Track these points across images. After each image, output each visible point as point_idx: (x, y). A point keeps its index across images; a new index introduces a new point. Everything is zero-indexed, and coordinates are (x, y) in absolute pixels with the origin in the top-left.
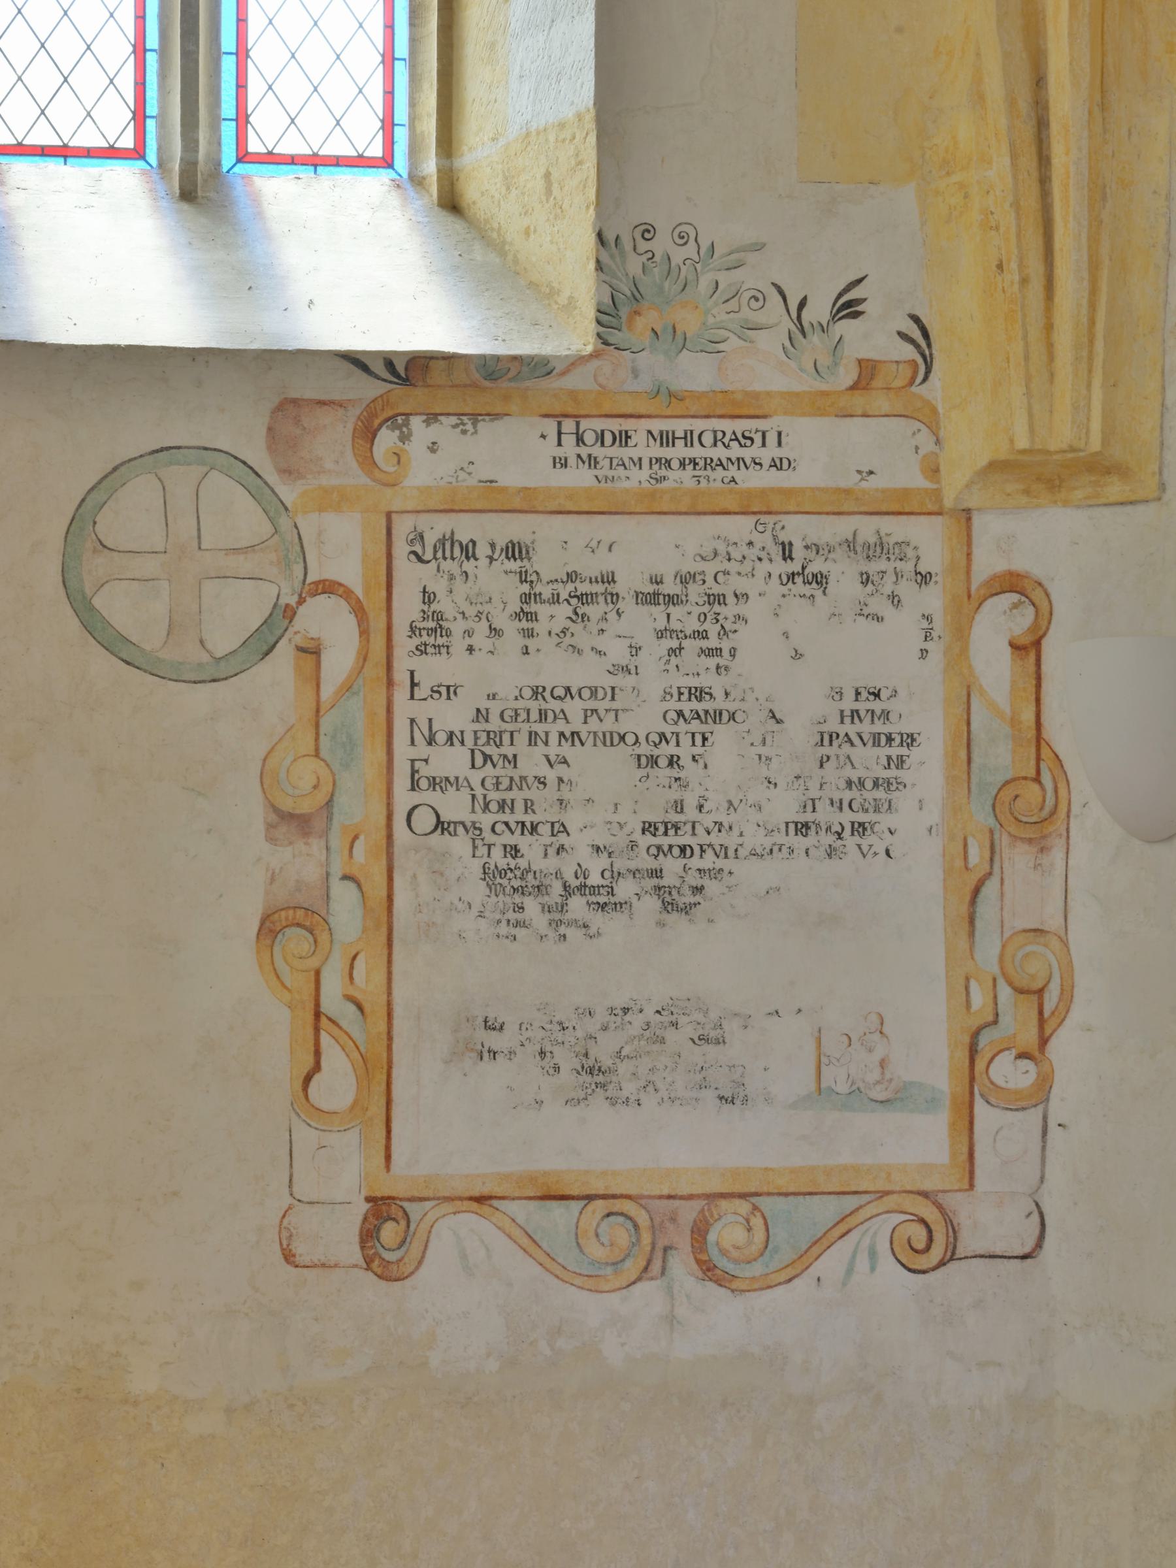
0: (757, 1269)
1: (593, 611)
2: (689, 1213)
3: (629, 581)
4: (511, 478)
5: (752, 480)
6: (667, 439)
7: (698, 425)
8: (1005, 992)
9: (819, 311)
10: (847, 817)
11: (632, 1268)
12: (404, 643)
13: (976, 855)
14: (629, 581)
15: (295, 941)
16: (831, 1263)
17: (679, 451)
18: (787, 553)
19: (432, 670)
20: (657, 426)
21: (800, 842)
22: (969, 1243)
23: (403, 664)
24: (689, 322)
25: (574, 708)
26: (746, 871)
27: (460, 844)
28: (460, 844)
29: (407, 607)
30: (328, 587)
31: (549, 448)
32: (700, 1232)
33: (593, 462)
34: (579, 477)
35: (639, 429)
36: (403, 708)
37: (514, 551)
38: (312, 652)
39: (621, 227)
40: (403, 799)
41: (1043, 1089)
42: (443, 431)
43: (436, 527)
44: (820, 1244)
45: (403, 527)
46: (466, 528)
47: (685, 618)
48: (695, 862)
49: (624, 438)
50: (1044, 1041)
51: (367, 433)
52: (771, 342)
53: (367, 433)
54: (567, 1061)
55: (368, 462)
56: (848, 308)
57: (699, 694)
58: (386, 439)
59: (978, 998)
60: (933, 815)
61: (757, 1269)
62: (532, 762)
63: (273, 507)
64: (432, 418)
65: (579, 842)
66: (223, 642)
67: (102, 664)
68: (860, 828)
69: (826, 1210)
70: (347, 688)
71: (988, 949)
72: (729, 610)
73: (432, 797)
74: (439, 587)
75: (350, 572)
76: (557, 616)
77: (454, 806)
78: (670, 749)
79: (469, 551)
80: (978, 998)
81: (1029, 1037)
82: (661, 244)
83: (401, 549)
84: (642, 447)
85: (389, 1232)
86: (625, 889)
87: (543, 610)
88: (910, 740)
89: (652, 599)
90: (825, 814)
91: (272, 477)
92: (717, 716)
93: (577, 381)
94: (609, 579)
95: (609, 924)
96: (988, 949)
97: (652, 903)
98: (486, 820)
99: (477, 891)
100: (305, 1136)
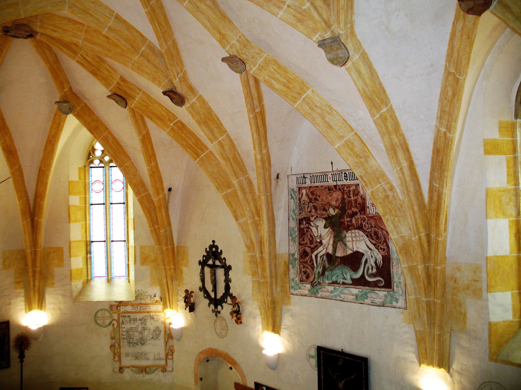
0: (150, 372)
1: (135, 321)
2: (144, 368)
3: (138, 319)
4: (129, 310)
5: (148, 310)
6: (141, 307)
7: (143, 306)
8: (169, 351)
9: (152, 296)
10: (156, 337)
11: (140, 372)
12: (121, 324)
13: (167, 340)
14: (138, 319)
15: (113, 348)
16: (156, 372)
17: (142, 308)
18: (151, 316)
19: (123, 326)
20: (140, 306)
21: (152, 339)
22: (167, 370)
23: (121, 326)
24: (142, 298)
25: (134, 329)
26: (150, 342)
27: (125, 340)
28: (125, 340)
29: (121, 321)
30: (114, 320)
31: (131, 308)
32: (145, 370)
33: (135, 309)
34: (134, 310)
35: (139, 306)
36: (121, 329)
37: (129, 316)
38: (113, 325)
39: (137, 290)
40: (121, 336)
41: (173, 358)
42: (123, 307)
43: (123, 315)
44: (155, 370)
45: (120, 315)
46: (125, 315)
47: (142, 321)
48: (144, 341)
49: (137, 307)
50: (173, 355)
51: (117, 307)
52: (149, 299)
53: (117, 307)
54: (134, 356)
55: (117, 310)
56: (155, 296)
57: (144, 327)
58: (119, 308)
59: (167, 351)
60: (163, 337)
61: (150, 372)
62: (131, 333)
63: (110, 314)
64: (122, 306)
65: (135, 339)
66: (107, 324)
67: (97, 326)
68: (157, 338)
69: (155, 368)
70: (116, 328)
71: (168, 347)
72: (146, 321)
73: (123, 336)
74: (123, 319)
75: (116, 318)
76: (132, 322)
77: (125, 337)
78: (141, 332)
79: (125, 316)
80: (167, 351)
81: (171, 354)
82: (140, 291)
83: (120, 317)
84: (139, 308)
85: (121, 370)
86: (138, 343)
87: (132, 321)
88: (161, 331)
89: (140, 320)
90: (154, 337)
91: (110, 311)
92: (145, 329)
93: (134, 302)
94: (136, 318)
95: (138, 346)
96: (168, 347)
97: (140, 345)
98: (128, 338)
99: (127, 344)
100: (115, 363)
